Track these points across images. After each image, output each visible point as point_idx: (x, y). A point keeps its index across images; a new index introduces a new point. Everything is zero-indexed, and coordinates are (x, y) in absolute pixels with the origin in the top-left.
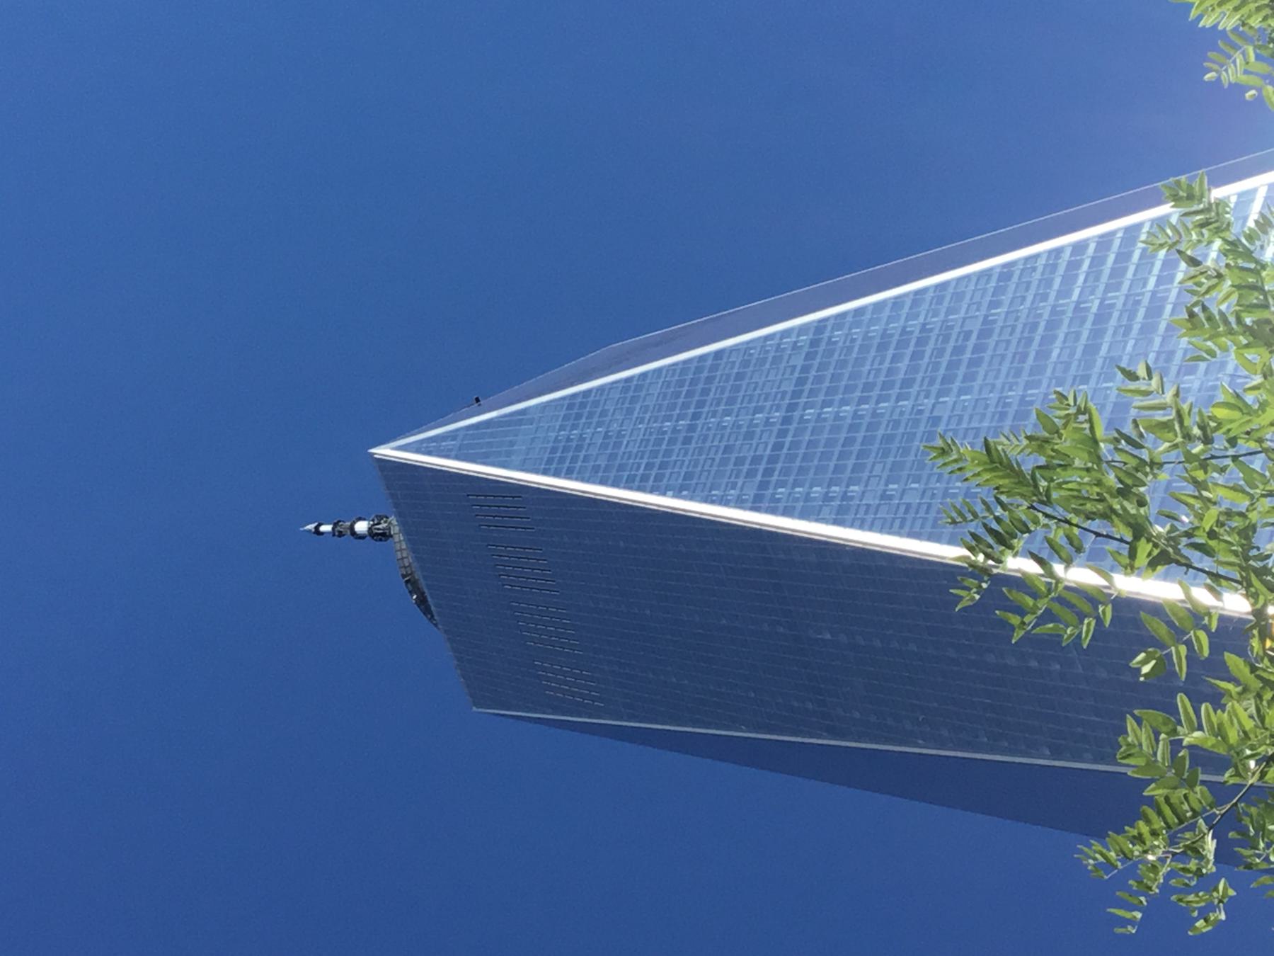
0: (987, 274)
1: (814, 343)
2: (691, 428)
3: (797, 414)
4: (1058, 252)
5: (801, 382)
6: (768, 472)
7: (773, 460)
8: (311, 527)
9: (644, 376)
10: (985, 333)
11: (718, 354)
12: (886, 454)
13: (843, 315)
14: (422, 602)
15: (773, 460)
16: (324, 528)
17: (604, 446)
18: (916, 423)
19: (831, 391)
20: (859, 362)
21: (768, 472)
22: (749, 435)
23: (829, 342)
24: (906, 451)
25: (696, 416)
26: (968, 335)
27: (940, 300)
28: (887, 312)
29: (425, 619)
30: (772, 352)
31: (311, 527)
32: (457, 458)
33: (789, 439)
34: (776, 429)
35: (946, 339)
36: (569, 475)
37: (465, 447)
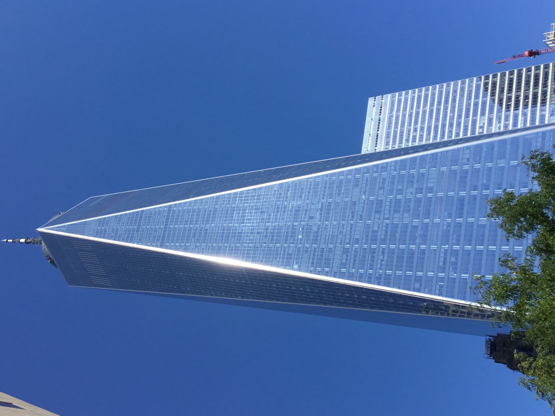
0: (213, 198)
1: (169, 210)
2: (138, 228)
3: (168, 227)
4: (230, 194)
5: (167, 219)
6: (163, 240)
7: (164, 237)
8: (5, 240)
9: (121, 215)
10: (215, 211)
11: (142, 211)
12: (195, 237)
13: (176, 204)
14: (52, 262)
15: (164, 237)
16: (9, 241)
17: (113, 232)
18: (201, 230)
19: (177, 222)
20: (183, 215)
21: (163, 240)
22: (155, 231)
23: (173, 210)
24: (200, 237)
25: (139, 225)
26: (210, 211)
27: (202, 203)
28: (188, 205)
29: (54, 267)
30: (158, 212)
31: (5, 240)
32: (67, 232)
33: (167, 232)
34: (163, 230)
35: (205, 212)
36: (104, 238)
37: (69, 229)
